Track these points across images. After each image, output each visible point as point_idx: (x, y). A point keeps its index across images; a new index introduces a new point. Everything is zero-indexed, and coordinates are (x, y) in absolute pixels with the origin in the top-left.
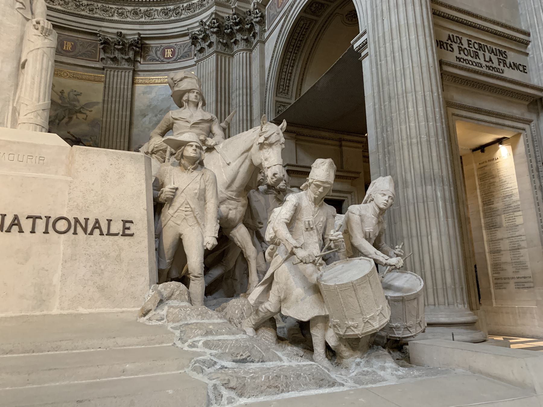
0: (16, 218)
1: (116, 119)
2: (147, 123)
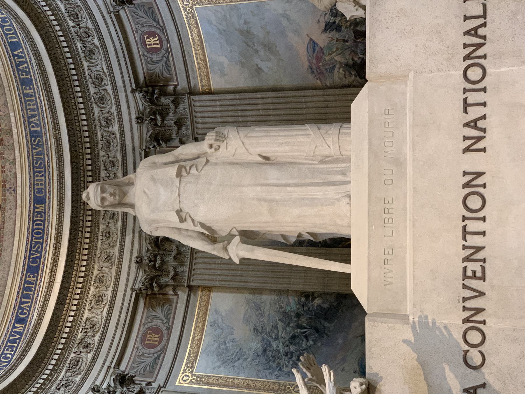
0: (467, 125)
1: (271, 112)
2: (270, 64)
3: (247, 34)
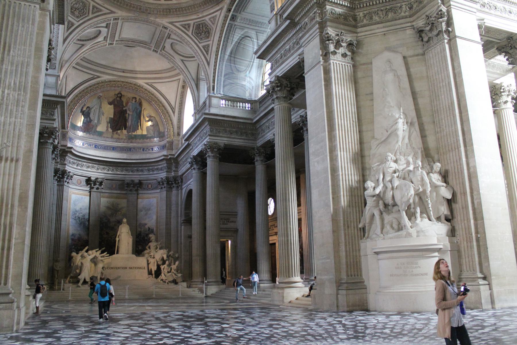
3: (149, 209)
